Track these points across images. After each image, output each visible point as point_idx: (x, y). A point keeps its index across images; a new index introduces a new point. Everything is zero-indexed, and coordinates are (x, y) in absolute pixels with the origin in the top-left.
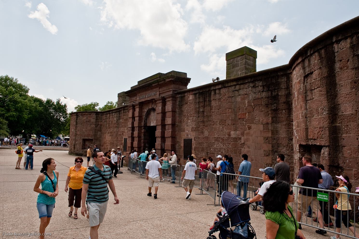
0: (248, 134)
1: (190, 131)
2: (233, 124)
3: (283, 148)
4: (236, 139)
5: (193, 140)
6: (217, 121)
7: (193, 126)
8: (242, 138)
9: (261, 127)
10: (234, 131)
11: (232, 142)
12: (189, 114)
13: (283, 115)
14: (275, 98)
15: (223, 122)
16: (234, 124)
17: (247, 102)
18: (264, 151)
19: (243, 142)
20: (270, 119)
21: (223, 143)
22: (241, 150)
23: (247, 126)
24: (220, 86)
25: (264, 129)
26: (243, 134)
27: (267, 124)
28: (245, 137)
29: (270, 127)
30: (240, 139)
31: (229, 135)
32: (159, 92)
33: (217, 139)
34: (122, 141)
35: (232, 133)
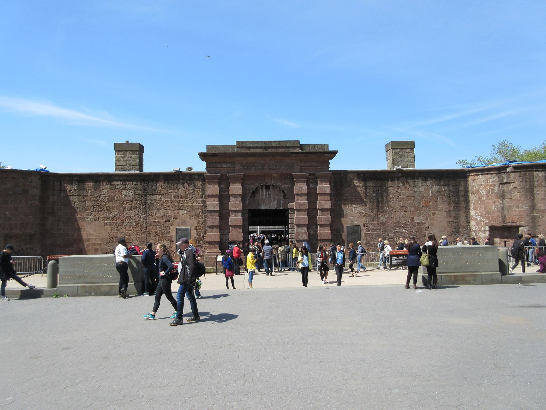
0: (432, 219)
1: (357, 216)
2: (416, 210)
3: (463, 229)
4: (420, 224)
5: (362, 227)
6: (397, 208)
7: (362, 211)
8: (427, 222)
9: (444, 214)
10: (418, 216)
11: (415, 226)
12: (354, 198)
13: (463, 205)
14: (457, 192)
15: (404, 208)
16: (417, 211)
17: (431, 192)
18: (448, 232)
19: (427, 225)
20: (452, 207)
21: (405, 228)
22: (426, 233)
23: (431, 213)
24: (400, 175)
25: (447, 215)
26: (427, 219)
27: (450, 211)
28: (430, 222)
29: (453, 214)
30: (424, 223)
31: (412, 220)
32: (301, 167)
33: (397, 225)
34: (299, 231)
35: (415, 218)
